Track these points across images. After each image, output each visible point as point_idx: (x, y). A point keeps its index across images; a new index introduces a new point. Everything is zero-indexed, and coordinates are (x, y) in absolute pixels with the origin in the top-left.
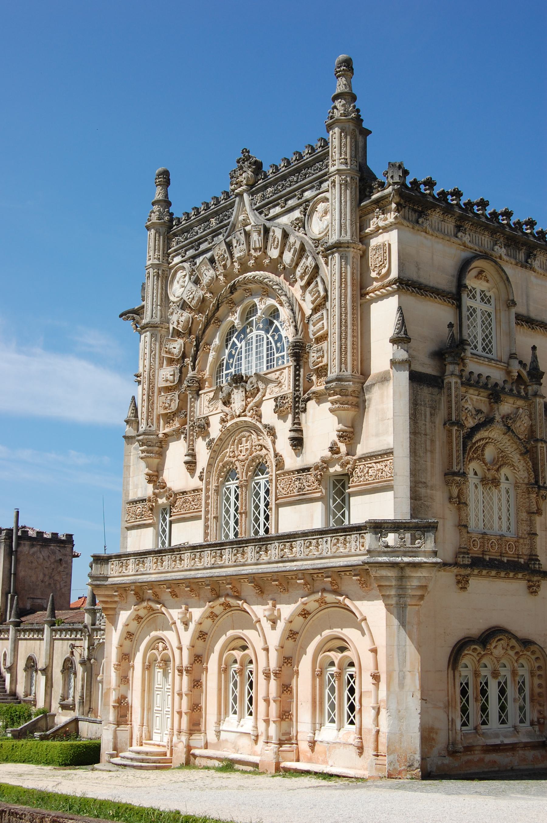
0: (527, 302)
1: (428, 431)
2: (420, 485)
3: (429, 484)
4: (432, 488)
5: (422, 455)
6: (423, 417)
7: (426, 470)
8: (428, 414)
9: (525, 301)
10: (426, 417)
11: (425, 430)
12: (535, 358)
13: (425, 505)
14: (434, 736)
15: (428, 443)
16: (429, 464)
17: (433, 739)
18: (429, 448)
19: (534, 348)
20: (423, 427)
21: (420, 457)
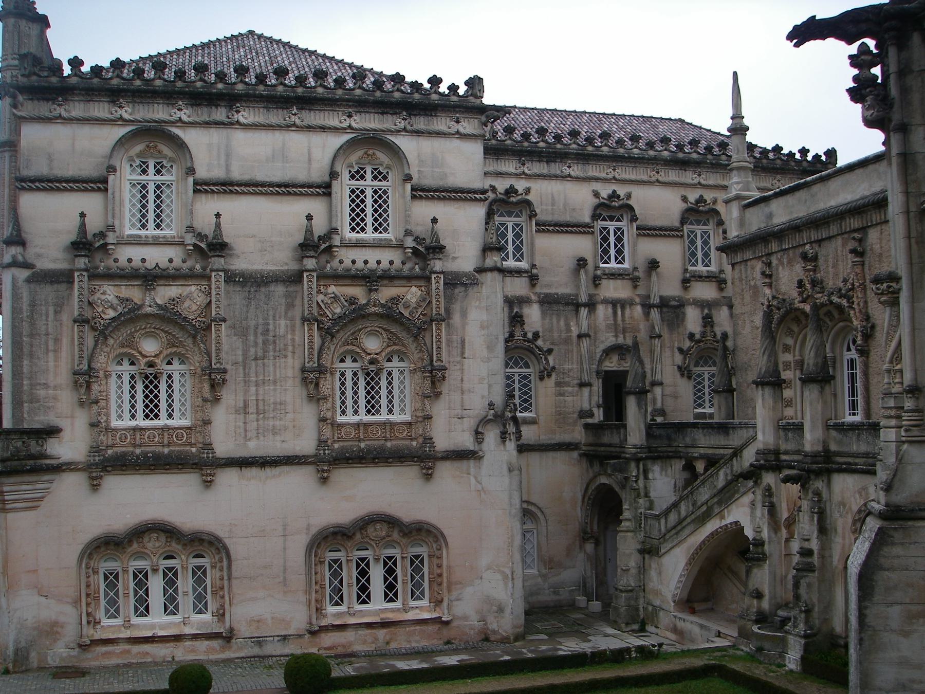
0: (227, 161)
1: (50, 330)
2: (38, 387)
3: (52, 385)
4: (55, 388)
5: (41, 356)
6: (44, 318)
7: (48, 370)
8: (51, 312)
9: (223, 162)
10: (47, 317)
11: (47, 329)
12: (218, 225)
13: (44, 407)
14: (59, 630)
15: (51, 343)
16: (51, 364)
17: (57, 633)
18: (51, 347)
19: (218, 215)
20: (44, 327)
21: (38, 358)
